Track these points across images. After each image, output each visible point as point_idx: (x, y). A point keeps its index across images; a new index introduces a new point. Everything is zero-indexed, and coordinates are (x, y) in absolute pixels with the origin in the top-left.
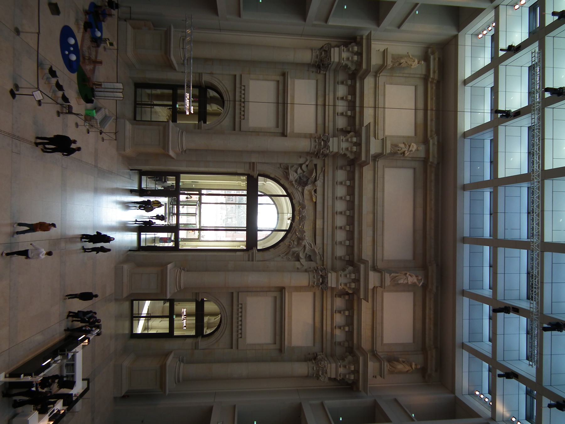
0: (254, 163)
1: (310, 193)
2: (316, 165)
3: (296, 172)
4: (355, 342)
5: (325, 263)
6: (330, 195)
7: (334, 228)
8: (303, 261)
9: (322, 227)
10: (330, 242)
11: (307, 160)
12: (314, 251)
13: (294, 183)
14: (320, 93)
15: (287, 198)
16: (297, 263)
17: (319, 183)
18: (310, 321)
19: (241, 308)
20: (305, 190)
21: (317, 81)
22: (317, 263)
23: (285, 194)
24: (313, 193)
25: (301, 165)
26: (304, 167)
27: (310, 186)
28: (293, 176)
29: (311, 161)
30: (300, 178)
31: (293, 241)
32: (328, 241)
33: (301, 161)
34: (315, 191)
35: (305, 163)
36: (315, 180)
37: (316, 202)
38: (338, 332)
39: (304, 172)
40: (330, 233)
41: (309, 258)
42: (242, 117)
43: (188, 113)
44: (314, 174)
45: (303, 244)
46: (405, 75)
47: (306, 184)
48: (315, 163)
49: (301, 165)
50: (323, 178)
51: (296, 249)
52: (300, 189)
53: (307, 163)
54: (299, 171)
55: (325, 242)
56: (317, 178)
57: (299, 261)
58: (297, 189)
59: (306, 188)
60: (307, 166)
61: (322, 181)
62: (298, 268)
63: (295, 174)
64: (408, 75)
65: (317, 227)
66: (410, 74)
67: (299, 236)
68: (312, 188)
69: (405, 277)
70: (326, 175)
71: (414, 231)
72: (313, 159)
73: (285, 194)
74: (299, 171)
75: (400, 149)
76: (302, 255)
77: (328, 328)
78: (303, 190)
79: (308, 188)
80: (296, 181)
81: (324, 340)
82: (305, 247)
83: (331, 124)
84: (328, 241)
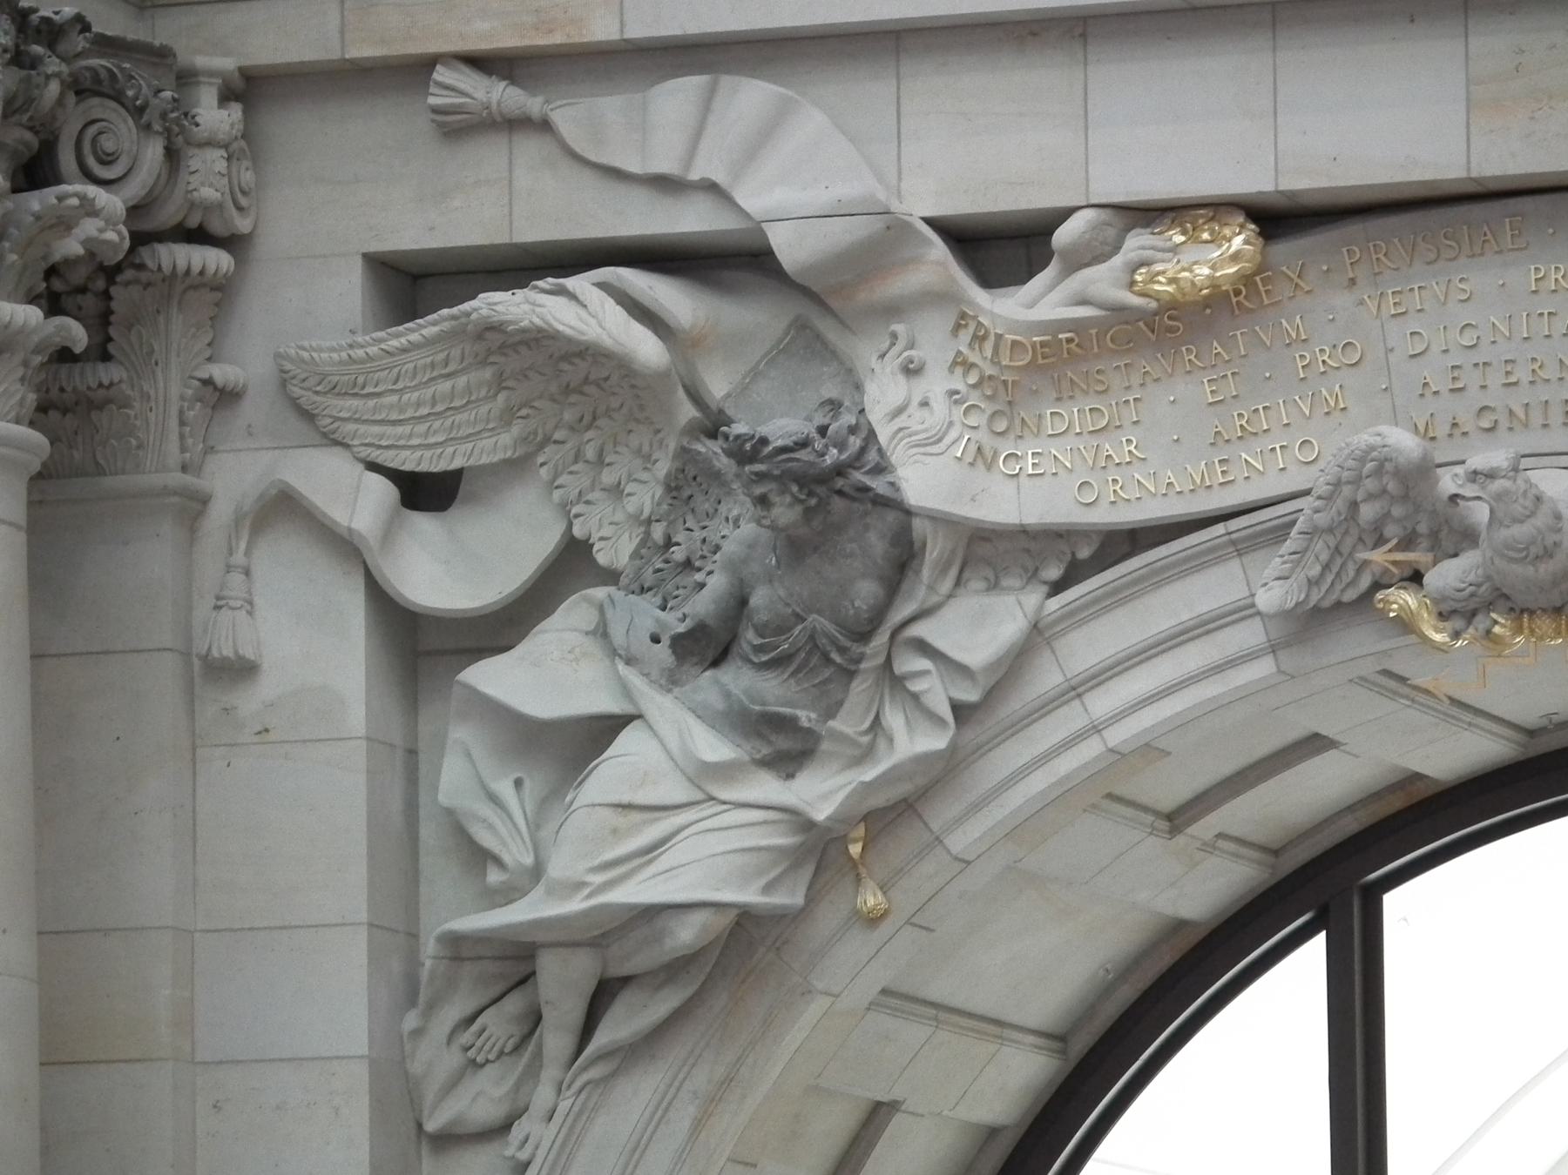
1: (1062, 359)
11: (283, 508)
13: (822, 792)
17: (799, 172)
20: (1004, 502)
24: (1037, 303)
25: (422, 648)
27: (883, 392)
28: (675, 818)
29: (307, 413)
30: (705, 646)
33: (309, 646)
34: (1000, 247)
36: (729, 262)
37: (1275, 219)
39: (571, 565)
44: (583, 310)
47: (832, 491)
48: (348, 291)
49: (422, 648)
50: (675, 98)
52: (976, 627)
53: (363, 504)
54: (544, 676)
56: (687, 220)
59: (923, 481)
60: (425, 492)
61: (749, 97)
63: (626, 766)
68: (933, 340)
72: (246, 362)
78: (989, 551)
80: (784, 745)
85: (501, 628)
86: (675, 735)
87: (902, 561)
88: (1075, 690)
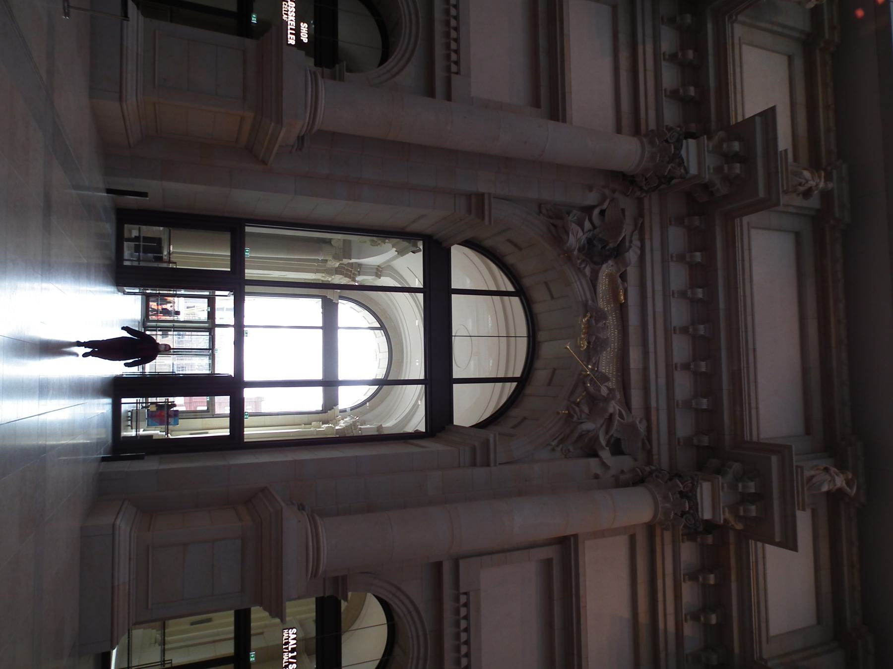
0: (481, 196)
2: (623, 210)
3: (582, 226)
4: (737, 650)
5: (655, 457)
6: (659, 287)
7: (670, 368)
8: (605, 454)
9: (641, 366)
10: (663, 405)
12: (633, 427)
13: (576, 253)
14: (623, 38)
15: (516, 301)
16: (593, 461)
17: (632, 256)
18: (625, 612)
19: (466, 605)
20: (600, 274)
21: (614, 8)
22: (635, 460)
23: (511, 288)
24: (619, 281)
25: (588, 210)
26: (596, 212)
28: (576, 237)
30: (590, 241)
31: (578, 404)
32: (659, 402)
33: (591, 199)
34: (623, 277)
35: (602, 202)
38: (689, 629)
39: (594, 227)
40: (662, 381)
41: (617, 448)
42: (454, 68)
43: (292, 42)
45: (611, 410)
46: (775, 28)
50: (638, 243)
51: (588, 426)
52: (588, 271)
53: (604, 207)
55: (653, 404)
57: (596, 455)
58: (580, 271)
59: (604, 266)
60: (602, 213)
61: (639, 252)
62: (597, 477)
63: (580, 233)
64: (779, 29)
65: (632, 365)
66: (784, 26)
67: (592, 390)
69: (828, 477)
70: (647, 236)
71: (805, 371)
72: (617, 195)
73: (511, 288)
74: (587, 225)
75: (803, 181)
76: (603, 440)
77: (668, 622)
79: (606, 269)
80: (580, 250)
81: (662, 655)
82: (611, 416)
83: (652, 114)
84: (659, 402)
85: (591, 221)
86: (583, 237)
87: (595, 263)
88: (579, 279)
